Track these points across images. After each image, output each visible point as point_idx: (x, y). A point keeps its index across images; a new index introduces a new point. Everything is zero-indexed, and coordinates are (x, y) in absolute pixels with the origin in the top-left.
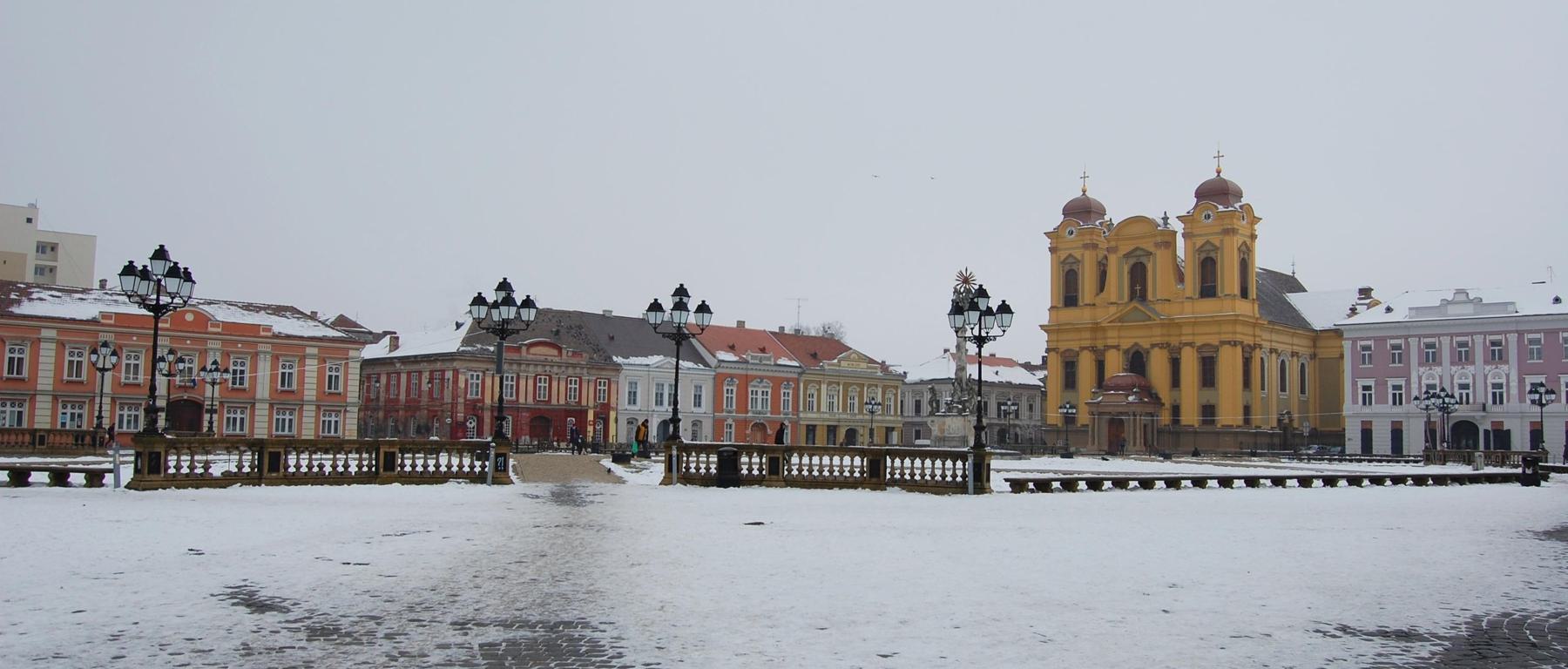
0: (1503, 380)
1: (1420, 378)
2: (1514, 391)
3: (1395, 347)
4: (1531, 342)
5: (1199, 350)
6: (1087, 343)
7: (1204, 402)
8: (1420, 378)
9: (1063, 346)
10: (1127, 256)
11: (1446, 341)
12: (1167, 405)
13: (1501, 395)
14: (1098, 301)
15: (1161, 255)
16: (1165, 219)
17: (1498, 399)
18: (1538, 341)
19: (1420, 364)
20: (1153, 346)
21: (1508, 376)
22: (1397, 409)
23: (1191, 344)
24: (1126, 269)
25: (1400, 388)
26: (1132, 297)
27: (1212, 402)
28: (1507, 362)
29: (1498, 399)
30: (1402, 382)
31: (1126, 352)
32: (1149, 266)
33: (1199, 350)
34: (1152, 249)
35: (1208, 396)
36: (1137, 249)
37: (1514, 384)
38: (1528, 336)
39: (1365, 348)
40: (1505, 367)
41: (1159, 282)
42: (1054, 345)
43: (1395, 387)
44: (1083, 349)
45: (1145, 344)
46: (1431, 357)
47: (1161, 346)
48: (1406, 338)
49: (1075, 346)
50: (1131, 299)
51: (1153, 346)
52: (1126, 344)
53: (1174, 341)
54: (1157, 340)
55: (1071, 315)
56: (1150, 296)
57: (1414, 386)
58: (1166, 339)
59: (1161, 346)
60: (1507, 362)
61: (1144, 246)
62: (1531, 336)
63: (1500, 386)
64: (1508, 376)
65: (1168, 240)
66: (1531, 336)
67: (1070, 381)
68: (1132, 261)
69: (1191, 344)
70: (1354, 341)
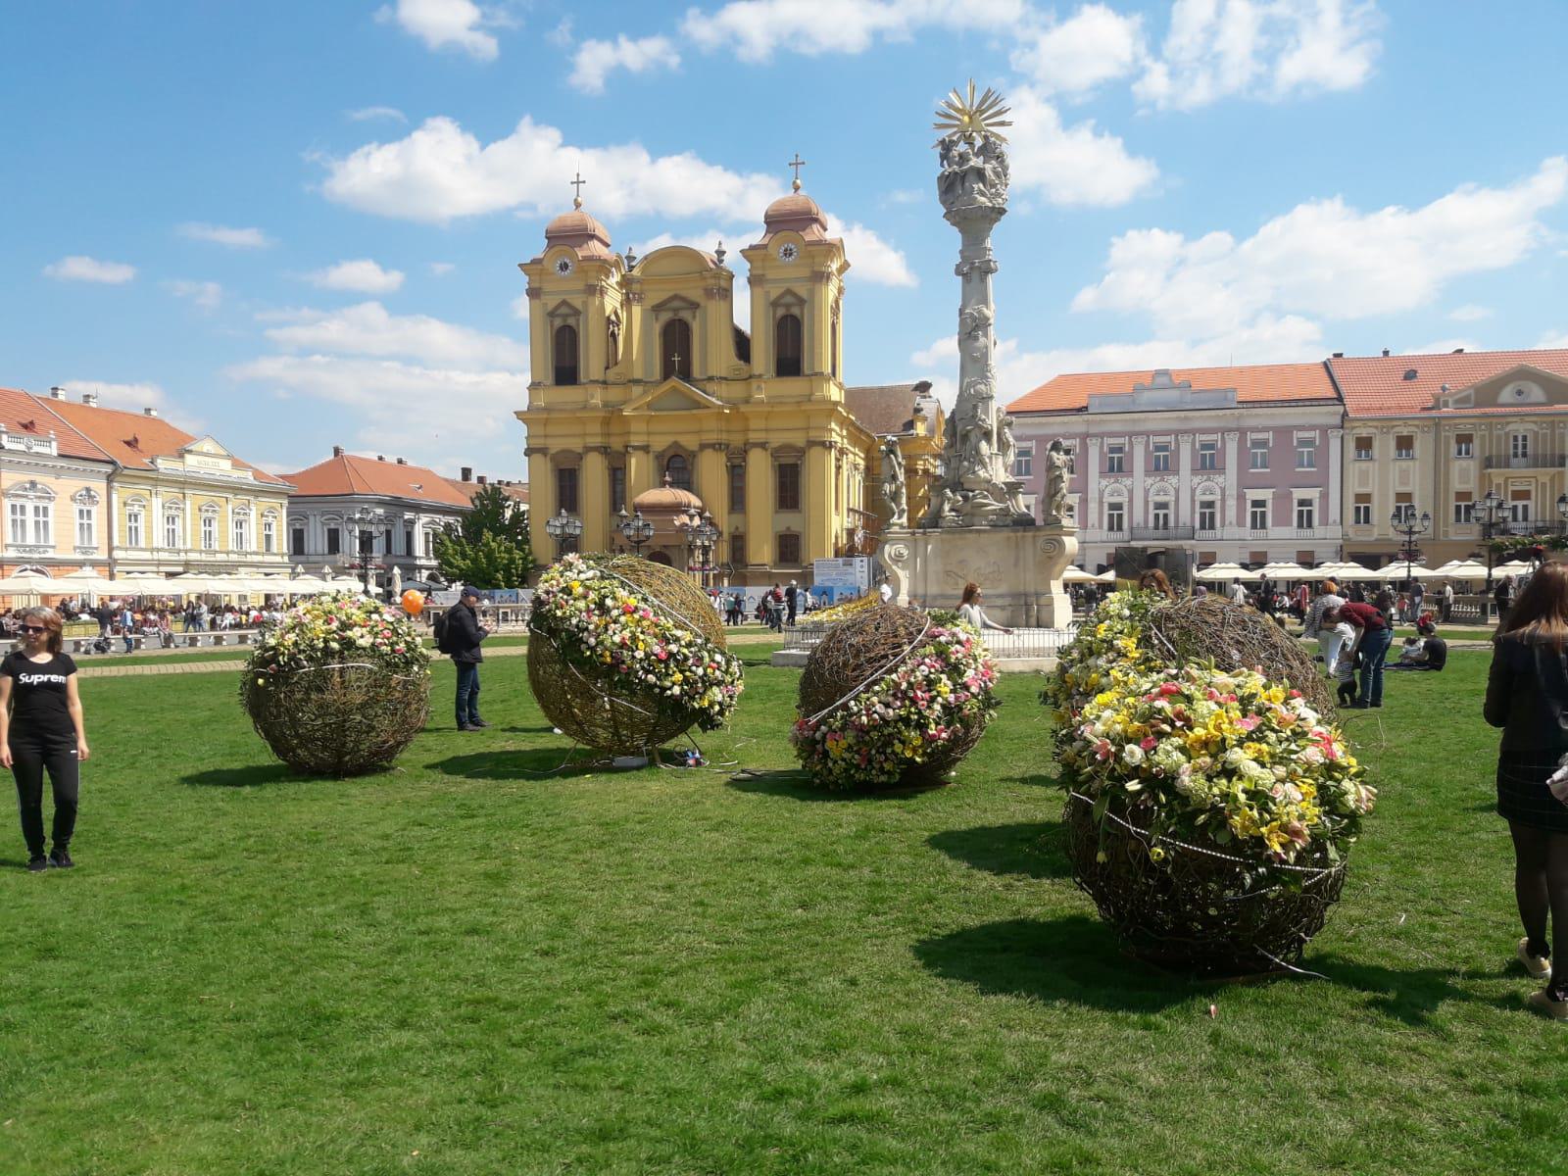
1: (1101, 494)
2: (1231, 513)
4: (1257, 444)
5: (776, 453)
6: (596, 441)
7: (781, 529)
9: (556, 445)
10: (657, 309)
12: (726, 536)
13: (1212, 515)
14: (611, 375)
15: (714, 307)
16: (721, 253)
17: (1208, 522)
18: (1263, 444)
19: (1102, 474)
20: (703, 447)
23: (763, 446)
24: (657, 328)
26: (667, 374)
27: (795, 528)
29: (1208, 522)
31: (659, 456)
32: (695, 327)
33: (776, 453)
34: (698, 300)
35: (790, 521)
36: (675, 297)
37: (1232, 503)
41: (713, 355)
42: (539, 443)
43: (1302, 503)
44: (588, 449)
45: (690, 442)
46: (1116, 466)
47: (716, 447)
49: (576, 445)
50: (666, 376)
51: (703, 447)
52: (660, 443)
53: (737, 440)
54: (712, 438)
55: (568, 394)
56: (696, 372)
57: (1093, 506)
58: (724, 437)
59: (716, 447)
60: (1222, 470)
61: (684, 293)
62: (1255, 436)
63: (1118, 506)
65: (726, 294)
66: (1255, 436)
67: (568, 496)
68: (666, 316)
69: (763, 446)
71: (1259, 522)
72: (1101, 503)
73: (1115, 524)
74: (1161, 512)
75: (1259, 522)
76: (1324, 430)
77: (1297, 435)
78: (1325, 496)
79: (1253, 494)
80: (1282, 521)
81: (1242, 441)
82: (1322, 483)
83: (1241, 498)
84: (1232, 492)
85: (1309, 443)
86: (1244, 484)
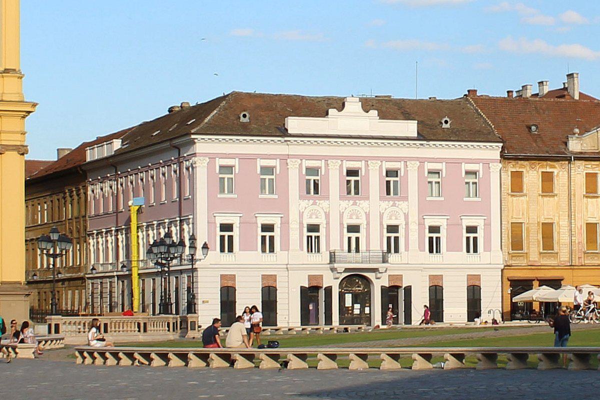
1: (301, 215)
2: (414, 236)
8: (301, 215)
17: (393, 246)
21: (406, 217)
28: (406, 199)
29: (393, 246)
30: (274, 220)
37: (414, 227)
39: (228, 169)
48: (284, 159)
57: (294, 226)
60: (406, 199)
64: (406, 217)
70: (212, 157)
71: (434, 246)
72: (301, 223)
73: (313, 245)
74: (354, 236)
75: (434, 246)
76: (486, 163)
78: (488, 225)
79: (430, 222)
81: (420, 169)
82: (486, 213)
83: (421, 224)
84: (414, 218)
86: (424, 209)
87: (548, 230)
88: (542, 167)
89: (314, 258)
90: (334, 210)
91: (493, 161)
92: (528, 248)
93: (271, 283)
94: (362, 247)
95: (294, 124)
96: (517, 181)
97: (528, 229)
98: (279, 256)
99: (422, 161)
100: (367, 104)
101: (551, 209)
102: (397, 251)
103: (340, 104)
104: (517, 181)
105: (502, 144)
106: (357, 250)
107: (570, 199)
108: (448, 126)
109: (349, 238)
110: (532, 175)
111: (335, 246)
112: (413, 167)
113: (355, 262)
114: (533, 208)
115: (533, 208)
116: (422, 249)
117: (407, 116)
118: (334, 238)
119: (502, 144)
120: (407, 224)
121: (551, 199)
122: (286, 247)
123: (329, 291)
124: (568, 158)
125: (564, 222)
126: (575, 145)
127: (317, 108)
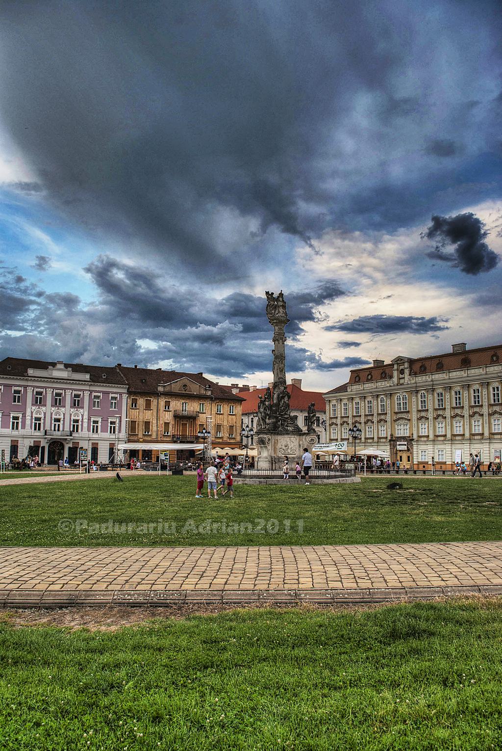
0: (80, 418)
1: (32, 413)
2: (85, 425)
3: (16, 392)
8: (32, 413)
11: (49, 391)
18: (98, 397)
21: (83, 416)
22: (15, 433)
25: (17, 418)
28: (83, 408)
29: (75, 428)
37: (86, 421)
38: (94, 394)
40: (82, 411)
48: (25, 387)
57: (28, 418)
60: (83, 408)
64: (83, 416)
71: (95, 430)
72: (32, 417)
73: (37, 427)
74: (57, 423)
76: (121, 394)
77: (111, 395)
80: (104, 430)
83: (89, 419)
84: (86, 416)
85: (115, 398)
87: (147, 424)
88: (146, 397)
89: (37, 433)
90: (48, 411)
91: (124, 393)
92: (138, 432)
93: (15, 444)
94: (61, 429)
95: (31, 372)
96: (135, 402)
97: (138, 424)
98: (21, 431)
99: (91, 392)
100: (67, 366)
101: (149, 415)
102: (77, 431)
103: (54, 365)
104: (135, 402)
105: (128, 386)
106: (59, 430)
107: (157, 412)
108: (105, 377)
109: (55, 425)
110: (141, 402)
111: (48, 428)
112: (87, 394)
113: (57, 435)
114: (142, 415)
115: (142, 415)
116: (89, 430)
117: (87, 372)
118: (48, 425)
119: (128, 386)
120: (82, 419)
121: (149, 411)
122: (23, 427)
123: (43, 448)
124: (157, 395)
125: (155, 422)
126: (160, 389)
127: (43, 365)
